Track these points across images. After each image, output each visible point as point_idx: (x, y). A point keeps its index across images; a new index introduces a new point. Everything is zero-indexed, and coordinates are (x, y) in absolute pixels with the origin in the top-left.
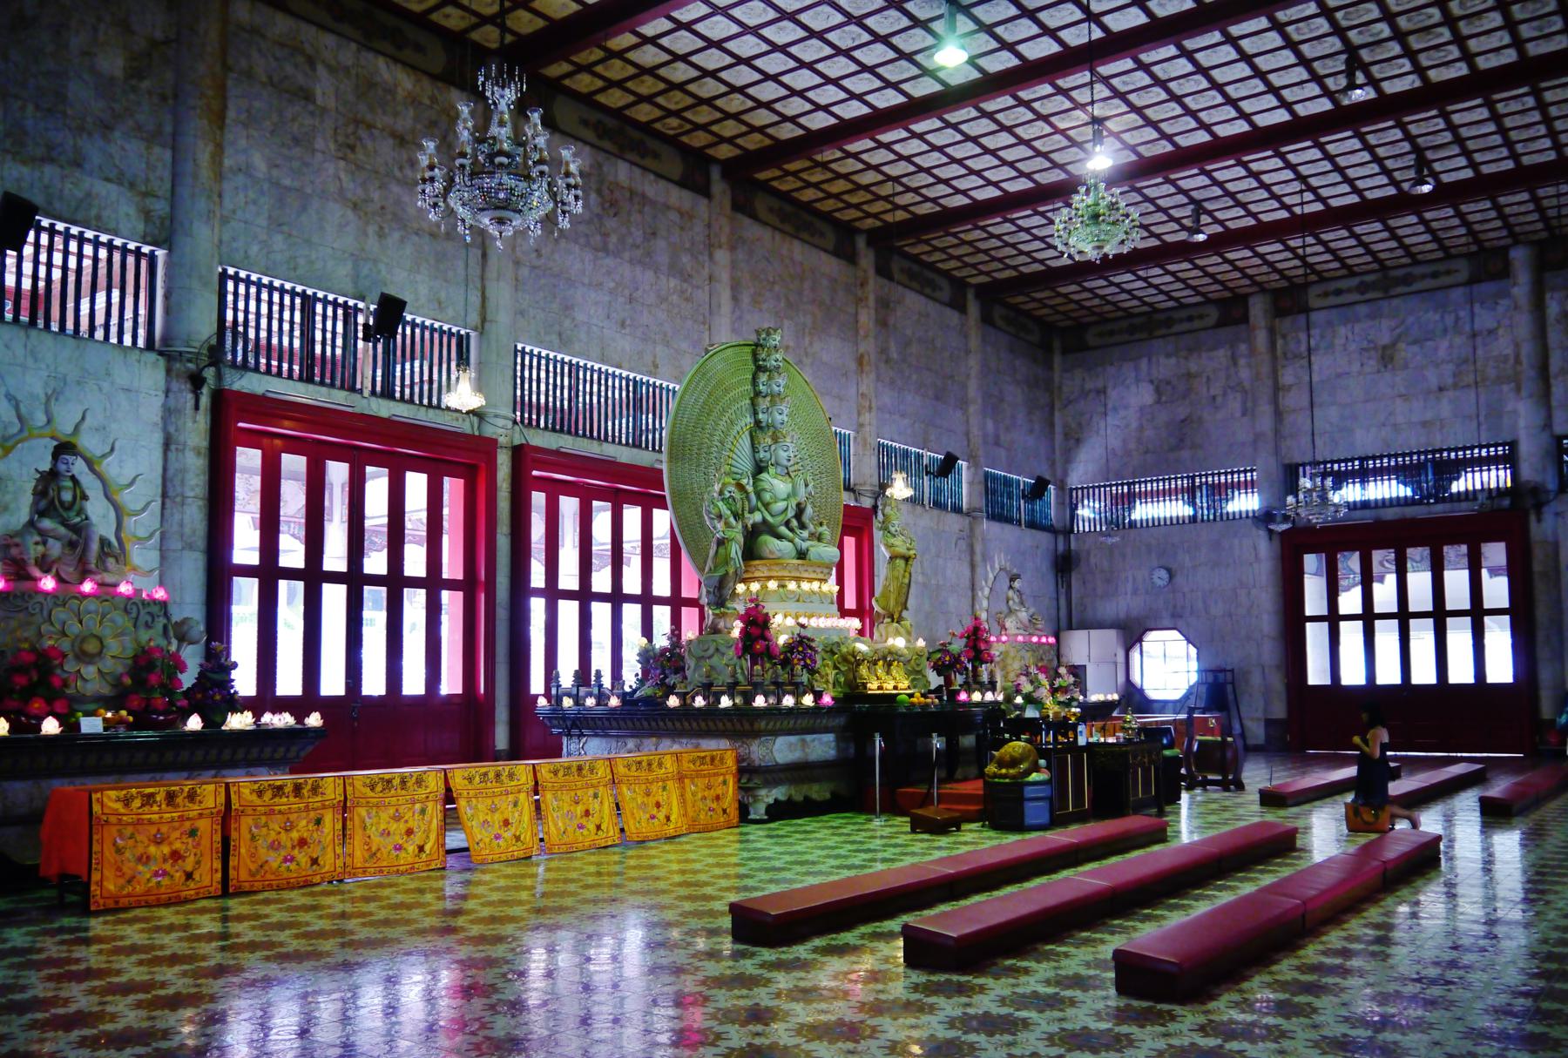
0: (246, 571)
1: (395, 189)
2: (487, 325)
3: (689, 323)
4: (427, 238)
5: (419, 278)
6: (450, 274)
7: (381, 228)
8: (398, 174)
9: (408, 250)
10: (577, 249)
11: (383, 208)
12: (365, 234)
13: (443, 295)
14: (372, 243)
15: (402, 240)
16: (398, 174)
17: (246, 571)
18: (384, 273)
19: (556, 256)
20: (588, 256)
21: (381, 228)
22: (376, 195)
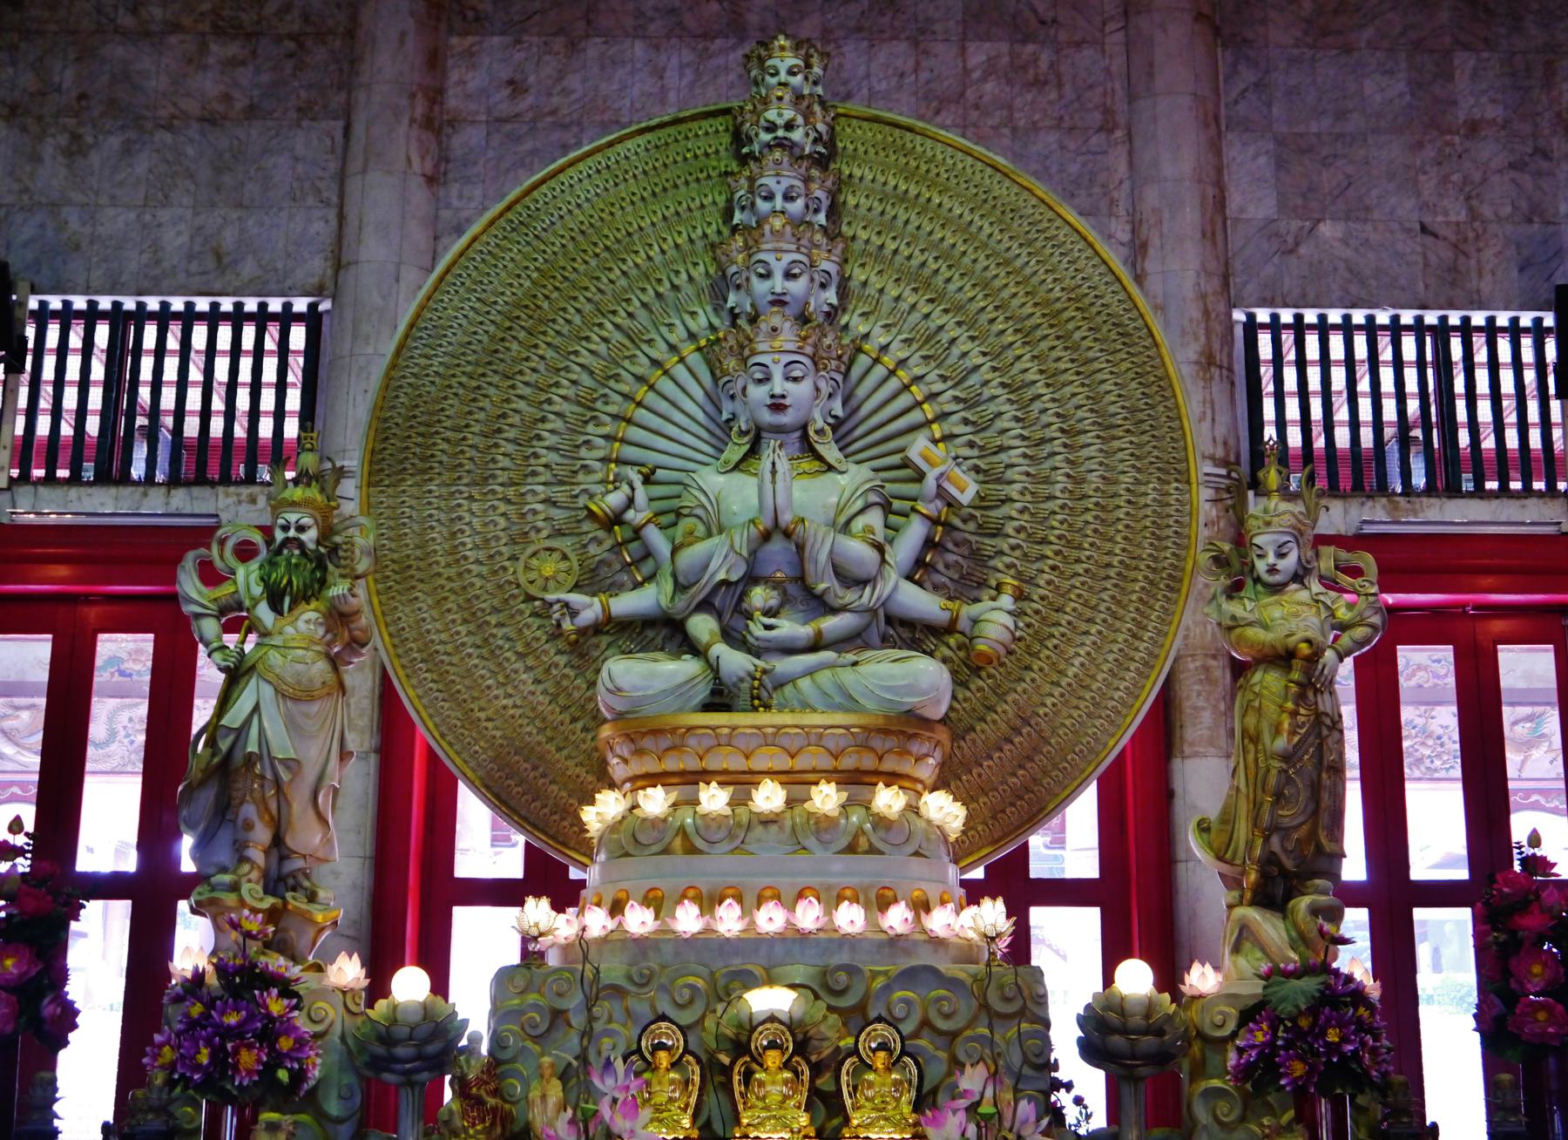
0: (1440, 894)
1: (118, 51)
2: (348, 277)
3: (1052, 138)
4: (193, 131)
5: (164, 215)
6: (252, 189)
7: (76, 137)
8: (127, 20)
9: (142, 164)
10: (639, 49)
11: (82, 97)
12: (36, 159)
13: (229, 237)
14: (52, 175)
15: (127, 150)
16: (127, 20)
17: (1440, 894)
18: (74, 224)
19: (573, 81)
20: (677, 58)
21: (76, 137)
22: (67, 77)
